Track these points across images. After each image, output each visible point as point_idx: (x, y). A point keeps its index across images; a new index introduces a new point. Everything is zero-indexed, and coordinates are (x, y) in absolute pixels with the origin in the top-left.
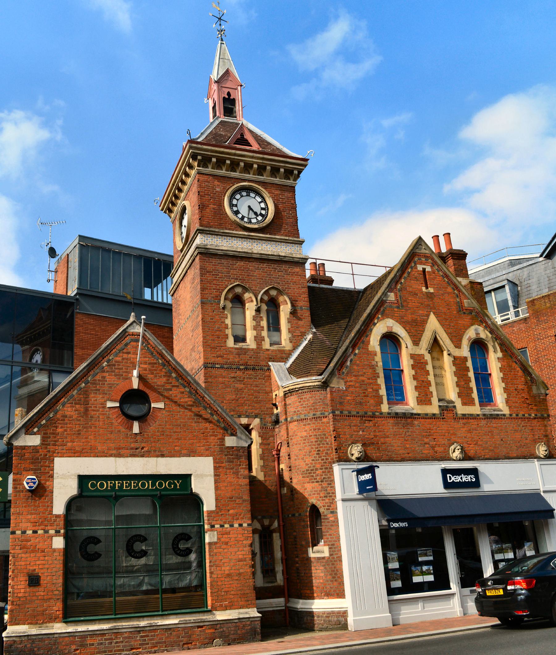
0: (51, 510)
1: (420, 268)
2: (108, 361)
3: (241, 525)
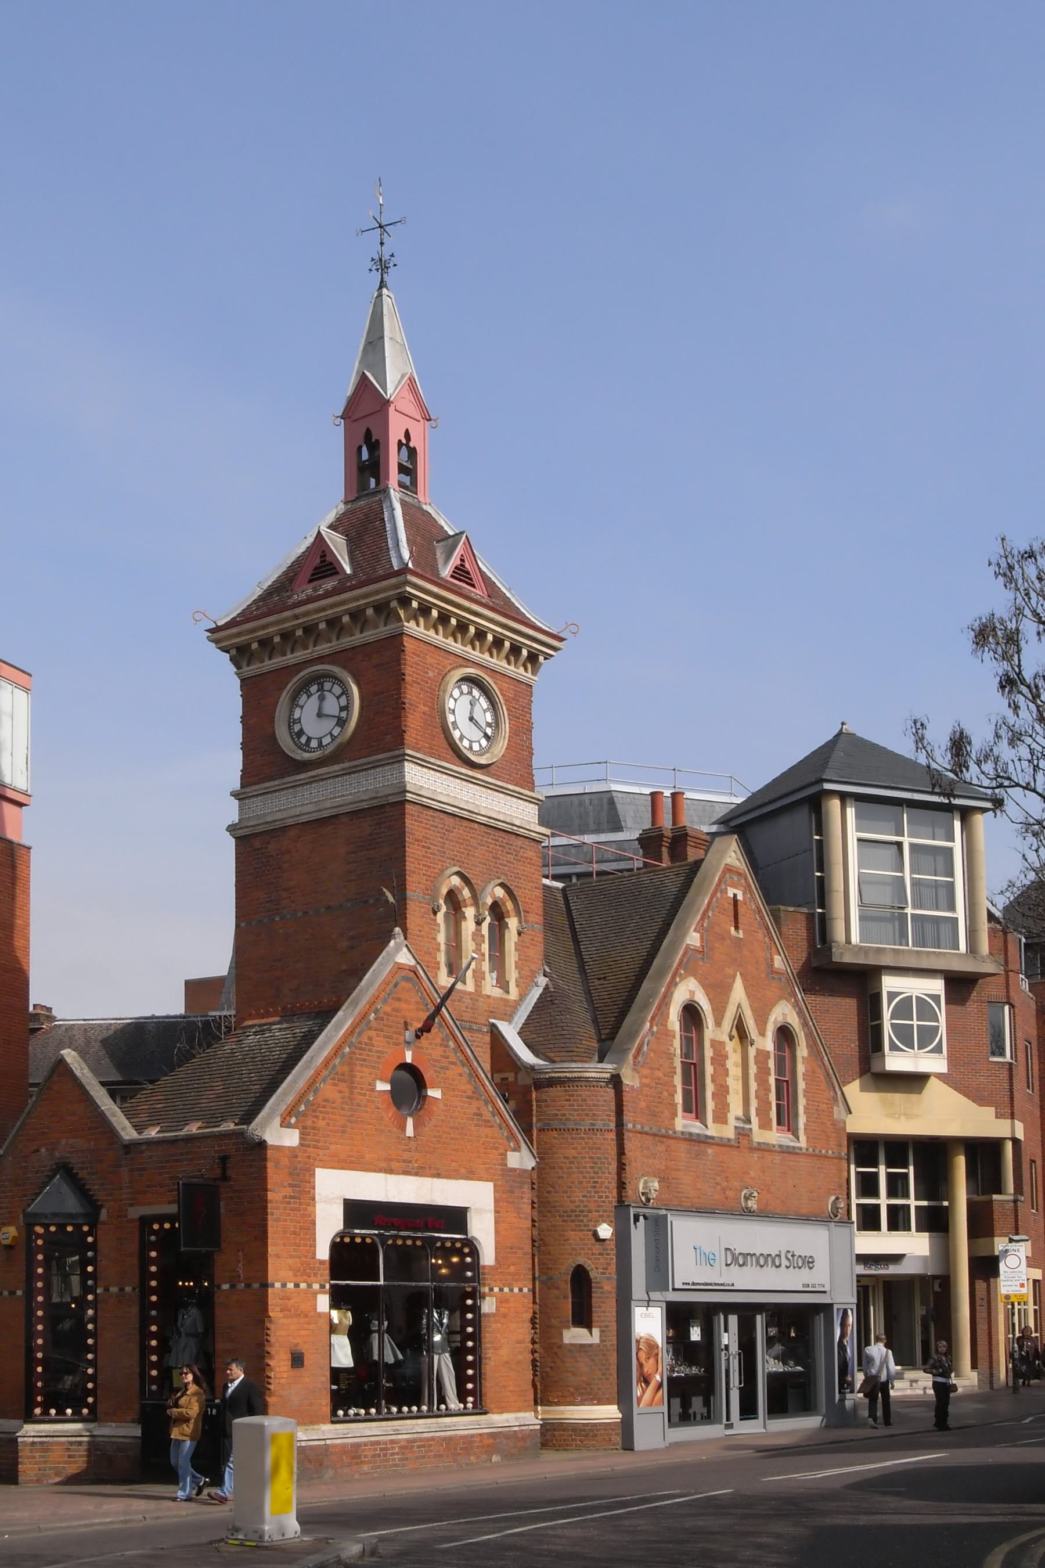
0: (314, 1254)
1: (731, 891)
2: (376, 1011)
3: (521, 1290)
